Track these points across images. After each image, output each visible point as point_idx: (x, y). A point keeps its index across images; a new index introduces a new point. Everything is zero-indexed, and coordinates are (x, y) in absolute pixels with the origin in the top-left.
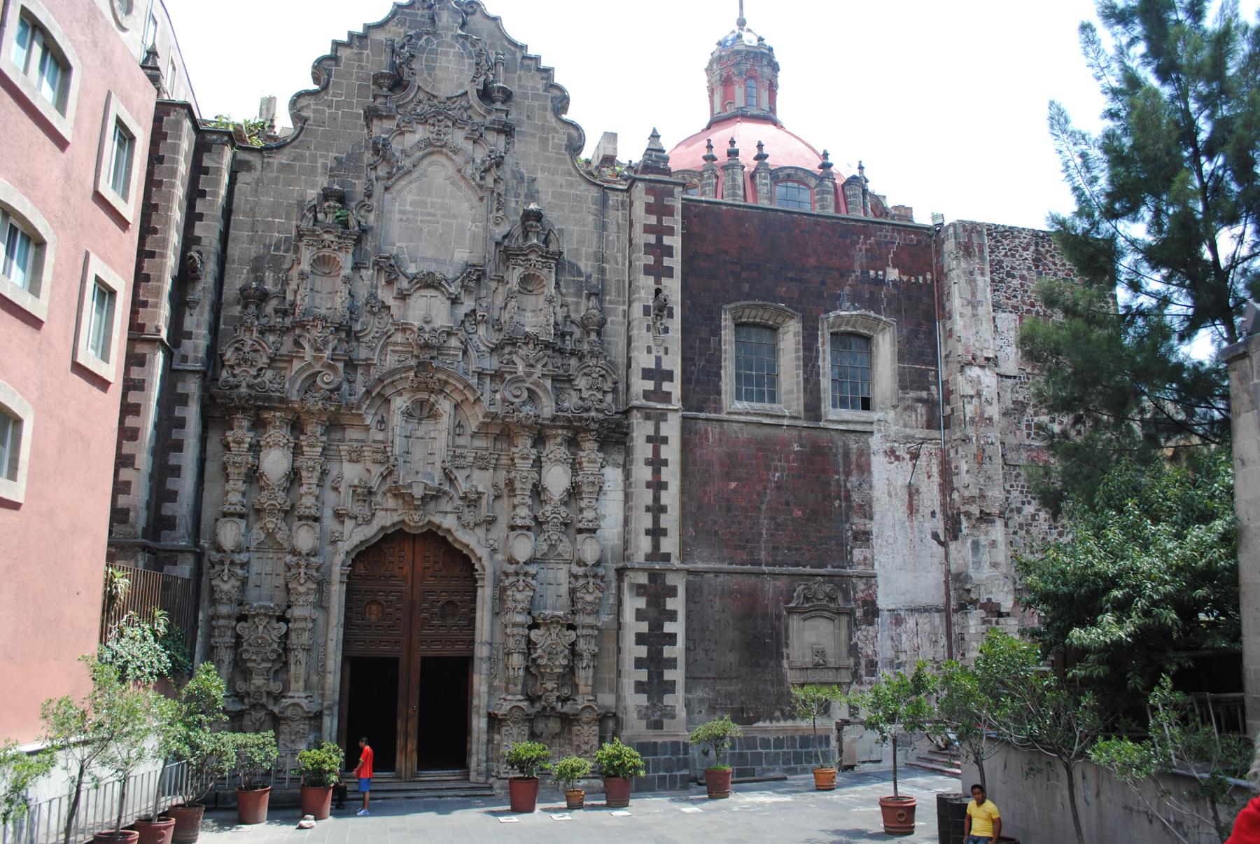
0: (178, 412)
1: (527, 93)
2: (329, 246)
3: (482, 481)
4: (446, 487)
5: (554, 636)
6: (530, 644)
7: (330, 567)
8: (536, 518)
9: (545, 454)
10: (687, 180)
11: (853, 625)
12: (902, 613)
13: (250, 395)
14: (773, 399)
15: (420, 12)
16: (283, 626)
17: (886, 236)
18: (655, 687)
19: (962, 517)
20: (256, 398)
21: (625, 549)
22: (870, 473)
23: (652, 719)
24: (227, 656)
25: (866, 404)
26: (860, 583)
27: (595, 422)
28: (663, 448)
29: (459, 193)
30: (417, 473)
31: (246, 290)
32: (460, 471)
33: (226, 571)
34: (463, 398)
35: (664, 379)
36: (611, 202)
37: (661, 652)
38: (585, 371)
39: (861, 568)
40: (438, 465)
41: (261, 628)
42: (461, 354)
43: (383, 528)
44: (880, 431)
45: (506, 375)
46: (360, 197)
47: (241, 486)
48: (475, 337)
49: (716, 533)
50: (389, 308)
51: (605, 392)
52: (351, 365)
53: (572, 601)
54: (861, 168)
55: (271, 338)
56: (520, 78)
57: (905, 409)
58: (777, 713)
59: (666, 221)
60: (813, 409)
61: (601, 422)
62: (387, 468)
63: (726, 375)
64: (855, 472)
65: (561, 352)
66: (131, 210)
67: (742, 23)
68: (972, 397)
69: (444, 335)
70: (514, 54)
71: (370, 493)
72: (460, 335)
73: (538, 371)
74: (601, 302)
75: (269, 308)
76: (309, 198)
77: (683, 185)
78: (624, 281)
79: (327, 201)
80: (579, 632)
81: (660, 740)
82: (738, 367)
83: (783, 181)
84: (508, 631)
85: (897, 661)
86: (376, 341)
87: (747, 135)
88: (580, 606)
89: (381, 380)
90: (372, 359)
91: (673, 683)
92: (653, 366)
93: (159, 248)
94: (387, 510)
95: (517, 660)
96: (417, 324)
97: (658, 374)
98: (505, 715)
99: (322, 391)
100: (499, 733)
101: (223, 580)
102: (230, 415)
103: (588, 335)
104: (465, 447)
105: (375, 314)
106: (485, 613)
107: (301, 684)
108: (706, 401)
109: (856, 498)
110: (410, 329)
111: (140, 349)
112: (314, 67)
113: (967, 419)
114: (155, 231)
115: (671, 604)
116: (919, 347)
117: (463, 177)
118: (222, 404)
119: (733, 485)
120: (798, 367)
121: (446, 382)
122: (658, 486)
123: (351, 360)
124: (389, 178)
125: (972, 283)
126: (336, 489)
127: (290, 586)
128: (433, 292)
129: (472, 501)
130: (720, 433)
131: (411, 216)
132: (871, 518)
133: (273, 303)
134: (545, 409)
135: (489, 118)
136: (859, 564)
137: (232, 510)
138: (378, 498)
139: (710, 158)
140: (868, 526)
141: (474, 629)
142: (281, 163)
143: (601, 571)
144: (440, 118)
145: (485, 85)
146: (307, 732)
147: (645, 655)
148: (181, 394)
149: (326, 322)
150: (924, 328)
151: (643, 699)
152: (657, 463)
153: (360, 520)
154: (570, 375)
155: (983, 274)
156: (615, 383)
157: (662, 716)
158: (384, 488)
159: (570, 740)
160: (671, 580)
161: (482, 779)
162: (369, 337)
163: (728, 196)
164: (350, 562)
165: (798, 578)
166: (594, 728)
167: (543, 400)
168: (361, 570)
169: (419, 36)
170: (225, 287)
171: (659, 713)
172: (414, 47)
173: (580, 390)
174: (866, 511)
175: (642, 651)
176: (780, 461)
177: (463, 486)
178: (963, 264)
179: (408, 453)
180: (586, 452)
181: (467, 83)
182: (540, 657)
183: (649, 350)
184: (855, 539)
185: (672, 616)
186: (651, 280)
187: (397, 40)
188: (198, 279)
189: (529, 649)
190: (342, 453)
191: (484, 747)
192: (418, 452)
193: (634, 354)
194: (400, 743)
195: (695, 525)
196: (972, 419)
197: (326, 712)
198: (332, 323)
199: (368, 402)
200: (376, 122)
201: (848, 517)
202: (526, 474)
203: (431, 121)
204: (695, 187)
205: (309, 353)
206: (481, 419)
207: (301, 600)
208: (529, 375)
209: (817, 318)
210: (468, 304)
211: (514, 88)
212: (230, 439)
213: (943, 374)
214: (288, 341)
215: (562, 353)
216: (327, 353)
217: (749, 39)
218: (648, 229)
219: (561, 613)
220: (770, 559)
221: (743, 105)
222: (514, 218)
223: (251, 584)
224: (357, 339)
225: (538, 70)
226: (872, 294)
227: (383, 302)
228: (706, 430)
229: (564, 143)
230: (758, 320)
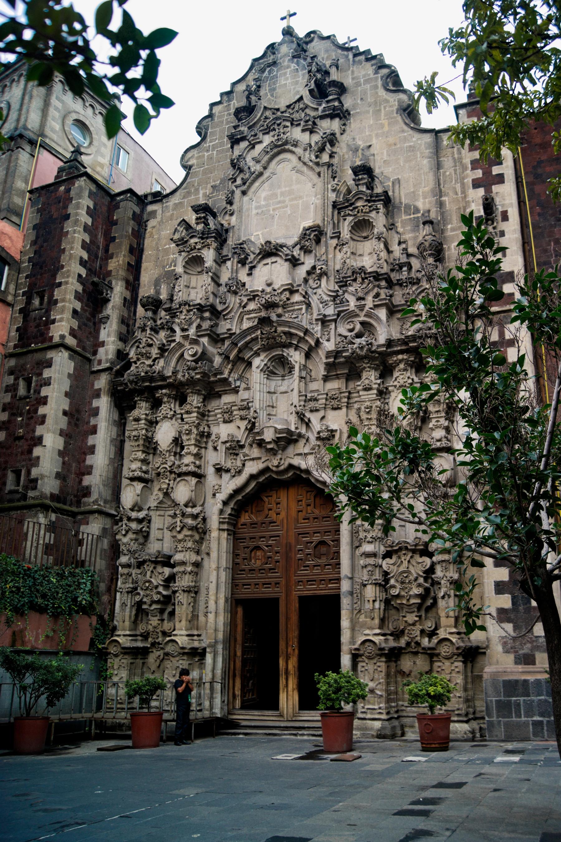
0: (95, 403)
1: (360, 82)
23: (521, 652)
29: (303, 178)
42: (304, 307)
43: (252, 477)
62: (250, 421)
69: (287, 293)
70: (347, 56)
72: (300, 291)
73: (369, 302)
80: (434, 559)
81: (531, 678)
94: (253, 459)
95: (370, 592)
110: (257, 295)
117: (305, 163)
121: (290, 335)
123: (218, 335)
124: (244, 184)
126: (215, 449)
128: (274, 259)
131: (264, 209)
135: (321, 108)
138: (246, 450)
147: (506, 578)
149: (189, 306)
157: (532, 649)
166: (456, 664)
171: (529, 645)
179: (273, 407)
181: (301, 89)
188: (107, 301)
198: (194, 305)
199: (230, 366)
206: (325, 361)
216: (192, 331)
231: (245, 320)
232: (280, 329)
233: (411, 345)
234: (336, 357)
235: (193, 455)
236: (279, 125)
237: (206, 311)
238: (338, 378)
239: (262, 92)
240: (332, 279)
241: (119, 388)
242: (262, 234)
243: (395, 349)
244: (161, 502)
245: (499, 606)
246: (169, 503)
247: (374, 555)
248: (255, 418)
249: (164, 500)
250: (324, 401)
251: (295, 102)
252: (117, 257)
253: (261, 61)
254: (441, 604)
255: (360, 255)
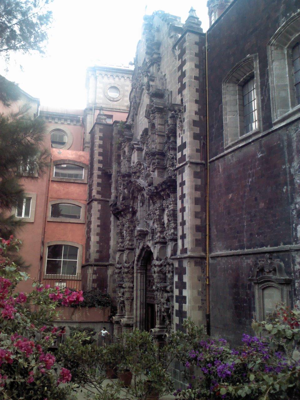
119: (230, 196)
176: (251, 169)
201: (293, 198)
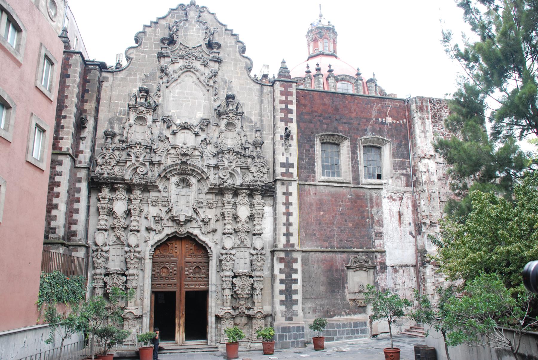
0: (78, 185)
1: (228, 45)
2: (142, 112)
3: (210, 214)
4: (195, 216)
5: (243, 281)
6: (233, 285)
7: (145, 252)
8: (234, 229)
9: (238, 201)
10: (297, 81)
11: (376, 273)
12: (397, 268)
13: (108, 177)
14: (338, 175)
15: (181, 12)
16: (124, 278)
17: (385, 104)
18: (289, 302)
19: (423, 225)
20: (111, 178)
21: (275, 242)
22: (382, 206)
23: (288, 316)
24: (100, 292)
25: (379, 177)
26: (378, 255)
27: (260, 186)
28: (290, 197)
30: (182, 210)
31: (106, 132)
32: (200, 209)
33: (99, 255)
34: (201, 177)
35: (290, 167)
36: (265, 91)
37: (291, 287)
38: (255, 164)
39: (379, 248)
40: (191, 207)
41: (115, 279)
42: (200, 158)
43: (167, 235)
44: (386, 188)
45: (220, 167)
46: (155, 91)
47: (106, 217)
48: (206, 151)
49: (315, 235)
50: (168, 138)
51: (264, 173)
52: (152, 163)
53: (252, 265)
54: (374, 75)
55: (117, 153)
56: (224, 38)
57: (396, 178)
58: (343, 313)
59: (289, 98)
60: (356, 178)
61: (262, 186)
62: (169, 209)
63: (317, 165)
64: (375, 206)
65: (244, 156)
66: (54, 97)
67: (321, 16)
68: (425, 172)
69: (193, 149)
70: (222, 28)
71: (162, 220)
72: (199, 150)
73: (234, 164)
74: (261, 134)
75: (116, 140)
76: (134, 92)
77: (296, 83)
78: (271, 125)
79: (141, 92)
80: (254, 279)
81: (291, 326)
82: (323, 161)
83: (340, 81)
84: (223, 279)
85: (395, 289)
86: (162, 153)
87: (324, 62)
88: (255, 268)
89: (165, 170)
90: (161, 161)
91: (297, 301)
92: (285, 161)
93: (68, 114)
94: (169, 227)
95: (228, 292)
96: (181, 145)
97: (287, 165)
98: (223, 316)
99: (140, 175)
100: (220, 324)
101: (98, 258)
102: (100, 187)
103: (256, 148)
104: (202, 199)
105: (162, 141)
106: (213, 271)
107: (133, 303)
108: (309, 177)
109: (376, 218)
110: (178, 147)
111: (60, 158)
112: (136, 36)
113: (423, 182)
114: (66, 107)
115: (295, 266)
116: (402, 151)
117: (200, 82)
118: (97, 181)
119: (322, 213)
120: (349, 161)
121: (193, 171)
122: (288, 214)
123: (152, 162)
124: (168, 83)
125: (423, 123)
127: (127, 260)
128: (187, 131)
129: (206, 222)
130: (315, 191)
131: (177, 99)
132: (383, 227)
133: (118, 138)
134: (237, 181)
135: (211, 56)
136: (378, 246)
137: (101, 227)
138: (165, 222)
139: (308, 72)
140: (381, 231)
141: (208, 279)
142: (121, 78)
143: (264, 252)
144: (190, 56)
145: (209, 41)
146: (136, 324)
147: (284, 288)
148: (79, 178)
149: (141, 145)
150: (403, 143)
151: (283, 308)
152: (288, 204)
153: (157, 231)
154: (248, 166)
155: (428, 119)
156: (268, 169)
157: (292, 315)
158: (168, 217)
159: (252, 326)
160: (295, 255)
161: (213, 344)
162: (160, 152)
163: (317, 88)
164: (153, 250)
165: (351, 253)
166: (262, 321)
167: (237, 177)
168: (158, 253)
169: (180, 22)
170: (98, 131)
171: (291, 314)
172: (177, 26)
173: (253, 173)
174: (380, 223)
175: (283, 287)
176: (342, 202)
177: (202, 216)
178: (419, 115)
180: (256, 200)
181: (201, 41)
182: (237, 290)
183: (283, 155)
184: (376, 235)
185: (296, 271)
186: (283, 124)
187: (171, 24)
188: (85, 127)
189: (233, 287)
190: (149, 202)
191: (214, 330)
192: (183, 201)
193: (276, 156)
194: (177, 329)
195: (305, 232)
196: (425, 182)
197: (144, 315)
199: (160, 180)
200: (162, 59)
202: (229, 210)
203: (186, 58)
204: (302, 84)
205: (133, 159)
206: (209, 186)
207: (132, 266)
208: (230, 166)
209: (357, 139)
210: (203, 136)
211: (222, 43)
212: (100, 197)
213: (412, 163)
214: (124, 153)
215: (245, 157)
216: (141, 159)
217: (324, 23)
218: (281, 102)
219: (246, 271)
220: (339, 245)
221: (322, 50)
222: (223, 98)
223: (110, 259)
224: (155, 152)
225: (232, 35)
226: (380, 128)
227: (166, 136)
228: (309, 190)
229: (244, 66)
230: (331, 141)
231: (169, 158)
232: (189, 167)
233: (251, 187)
234: (215, 186)
235: (137, 221)
236: (189, 57)
237: (148, 148)
238: (212, 194)
239: (179, 34)
240: (213, 145)
241: (95, 180)
242: (176, 112)
243: (243, 188)
244: (115, 242)
245: (281, 299)
246: (119, 243)
247: (229, 276)
248: (172, 207)
249: (117, 241)
250: (206, 204)
251: (197, 47)
252: (90, 102)
253: (175, 11)
254: (256, 297)
255: (227, 138)
